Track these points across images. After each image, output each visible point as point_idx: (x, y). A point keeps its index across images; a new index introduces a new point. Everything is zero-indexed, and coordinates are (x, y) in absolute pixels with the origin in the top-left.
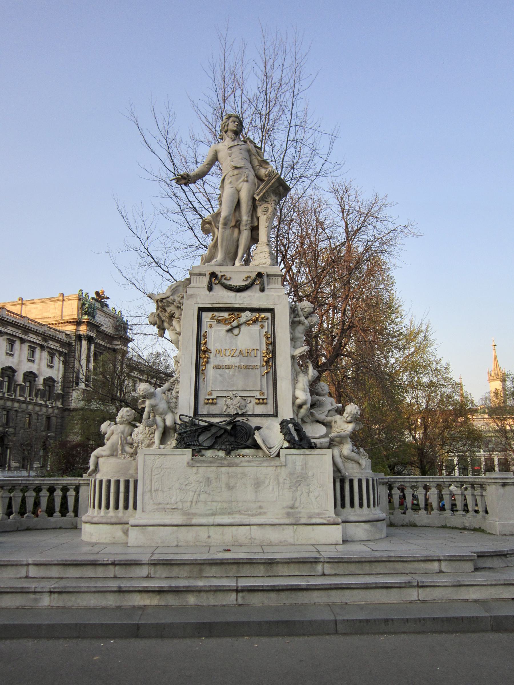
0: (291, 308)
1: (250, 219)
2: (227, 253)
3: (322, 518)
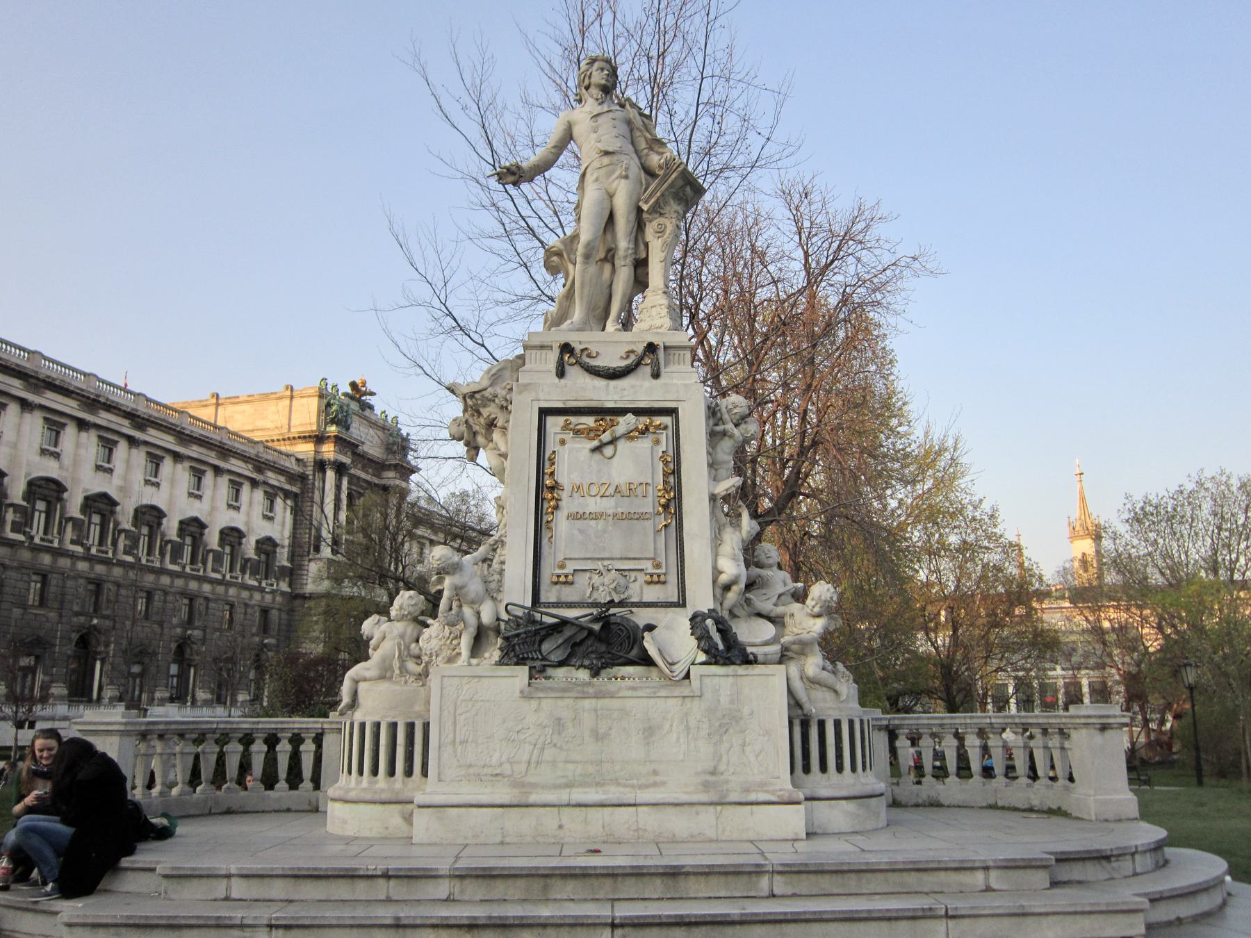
0: (709, 408)
1: (632, 246)
2: (590, 309)
3: (767, 791)
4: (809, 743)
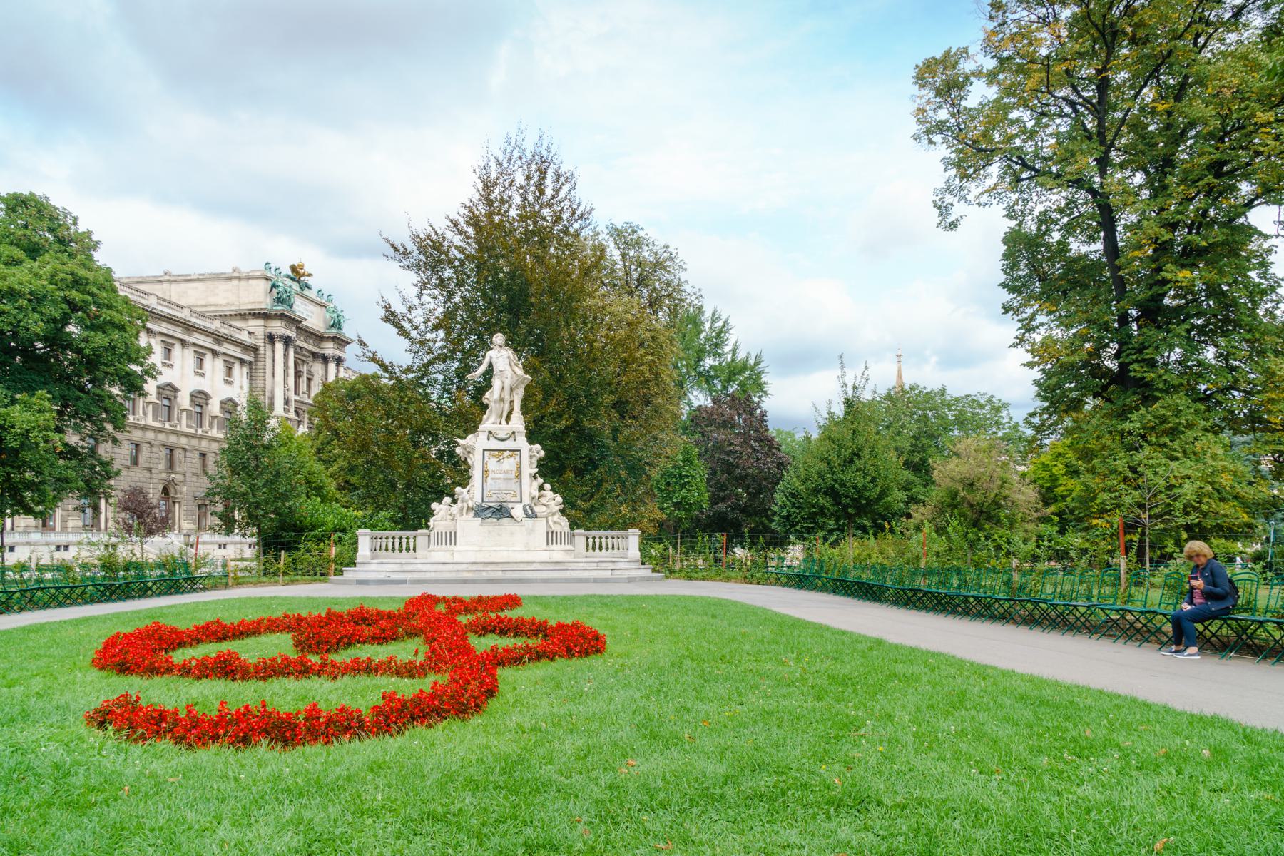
4: (551, 537)
